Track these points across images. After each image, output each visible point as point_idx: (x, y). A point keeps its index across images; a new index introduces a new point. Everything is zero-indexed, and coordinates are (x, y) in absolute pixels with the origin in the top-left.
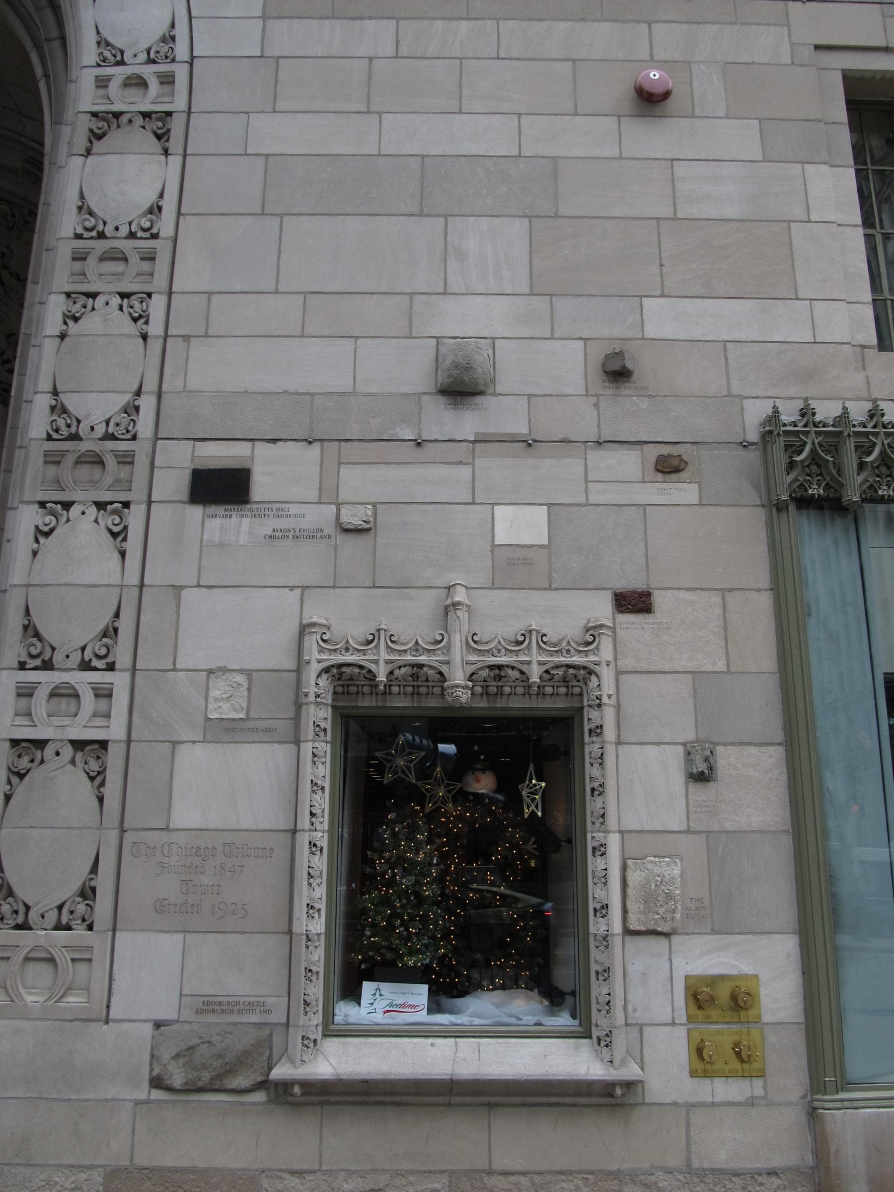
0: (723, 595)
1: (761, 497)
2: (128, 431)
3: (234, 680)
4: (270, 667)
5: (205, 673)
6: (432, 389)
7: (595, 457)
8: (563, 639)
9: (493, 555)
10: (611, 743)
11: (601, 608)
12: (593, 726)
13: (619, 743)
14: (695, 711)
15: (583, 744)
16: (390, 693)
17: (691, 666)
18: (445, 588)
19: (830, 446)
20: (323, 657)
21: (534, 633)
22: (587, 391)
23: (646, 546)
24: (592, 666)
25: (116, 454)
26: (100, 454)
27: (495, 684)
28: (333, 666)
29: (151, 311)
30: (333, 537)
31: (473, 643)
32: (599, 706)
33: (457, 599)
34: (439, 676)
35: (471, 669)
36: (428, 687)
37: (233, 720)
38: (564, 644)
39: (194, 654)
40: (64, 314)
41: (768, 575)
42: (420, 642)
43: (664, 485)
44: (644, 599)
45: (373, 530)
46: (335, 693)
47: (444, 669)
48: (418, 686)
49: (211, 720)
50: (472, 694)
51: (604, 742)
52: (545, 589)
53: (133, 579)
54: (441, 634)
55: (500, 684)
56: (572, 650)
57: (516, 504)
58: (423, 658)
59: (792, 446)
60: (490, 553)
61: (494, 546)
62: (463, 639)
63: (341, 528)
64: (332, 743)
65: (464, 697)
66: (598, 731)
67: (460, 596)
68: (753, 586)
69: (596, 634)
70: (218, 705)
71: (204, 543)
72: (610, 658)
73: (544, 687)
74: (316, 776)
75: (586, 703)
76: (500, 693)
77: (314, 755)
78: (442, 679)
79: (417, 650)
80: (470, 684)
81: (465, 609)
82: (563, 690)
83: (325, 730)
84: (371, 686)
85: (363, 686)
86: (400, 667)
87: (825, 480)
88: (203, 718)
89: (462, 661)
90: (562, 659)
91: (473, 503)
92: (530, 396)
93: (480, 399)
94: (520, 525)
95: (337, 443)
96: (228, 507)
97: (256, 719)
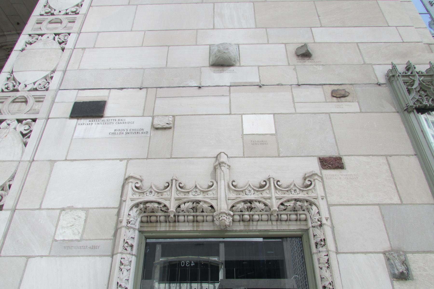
0: (387, 158)
1: (395, 108)
2: (45, 87)
3: (76, 215)
4: (101, 206)
5: (58, 211)
6: (207, 63)
7: (297, 91)
8: (291, 184)
9: (243, 139)
10: (333, 252)
11: (314, 166)
12: (318, 240)
13: (337, 253)
14: (386, 230)
15: (311, 254)
16: (178, 222)
17: (377, 200)
18: (214, 157)
19: (429, 82)
20: (135, 197)
21: (272, 180)
22: (289, 64)
23: (334, 133)
24: (313, 200)
25: (35, 97)
26: (27, 97)
27: (247, 213)
28: (141, 203)
29: (69, 40)
30: (149, 133)
31: (233, 186)
32: (321, 225)
33: (222, 160)
34: (210, 208)
35: (231, 203)
36: (203, 216)
37: (72, 240)
38: (292, 186)
39: (53, 200)
40: (26, 42)
41: (411, 147)
42: (198, 186)
43: (338, 103)
44: (338, 161)
45: (172, 129)
46: (142, 222)
47: (214, 203)
48: (197, 216)
49: (56, 241)
50: (233, 221)
51: (328, 251)
52: (276, 157)
53: (27, 157)
54: (211, 182)
55: (251, 213)
56: (298, 190)
57: (255, 114)
58: (200, 197)
59: (407, 82)
60: (241, 139)
61: (243, 135)
62: (226, 184)
63: (154, 127)
64: (137, 256)
65: (228, 221)
66: (323, 243)
67: (223, 158)
68: (404, 153)
69: (312, 180)
70: (64, 230)
71: (74, 138)
72: (323, 195)
73: (281, 215)
74: (121, 280)
75: (310, 225)
76: (251, 220)
77: (122, 264)
78: (213, 210)
79: (196, 192)
80: (232, 213)
81: (227, 166)
82: (293, 217)
83: (132, 246)
84: (165, 216)
85: (160, 216)
86: (185, 203)
87: (430, 98)
88: (51, 240)
89: (226, 197)
90: (291, 195)
91: (230, 114)
92: (259, 67)
93: (232, 68)
94: (259, 124)
95: (155, 89)
96: (91, 120)
97: (87, 240)
